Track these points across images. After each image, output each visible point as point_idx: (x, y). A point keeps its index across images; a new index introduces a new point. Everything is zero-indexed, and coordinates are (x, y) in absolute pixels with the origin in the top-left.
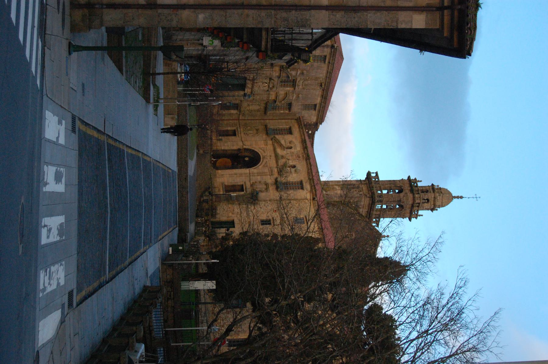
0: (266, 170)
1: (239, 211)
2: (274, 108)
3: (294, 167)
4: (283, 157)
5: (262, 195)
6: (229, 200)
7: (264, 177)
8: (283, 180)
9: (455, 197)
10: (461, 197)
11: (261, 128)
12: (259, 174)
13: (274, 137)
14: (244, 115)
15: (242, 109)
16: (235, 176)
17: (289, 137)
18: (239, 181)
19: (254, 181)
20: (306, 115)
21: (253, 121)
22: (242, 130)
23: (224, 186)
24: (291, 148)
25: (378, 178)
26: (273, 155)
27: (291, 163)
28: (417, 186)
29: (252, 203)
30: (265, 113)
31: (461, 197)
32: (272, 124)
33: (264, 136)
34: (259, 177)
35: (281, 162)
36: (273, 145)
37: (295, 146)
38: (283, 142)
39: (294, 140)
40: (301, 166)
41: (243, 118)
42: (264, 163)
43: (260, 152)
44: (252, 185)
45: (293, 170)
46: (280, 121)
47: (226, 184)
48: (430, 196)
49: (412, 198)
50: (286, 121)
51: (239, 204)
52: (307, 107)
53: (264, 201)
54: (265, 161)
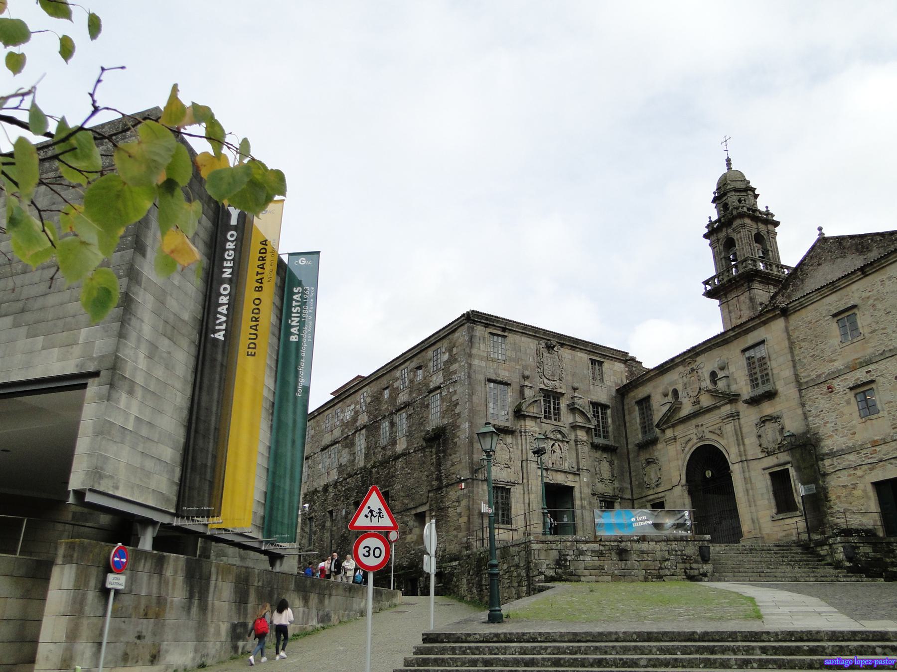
0: (729, 428)
3: (713, 375)
5: (793, 425)
6: (818, 503)
7: (745, 430)
8: (745, 390)
9: (729, 168)
10: (728, 161)
11: (643, 456)
13: (658, 426)
14: (621, 490)
15: (611, 493)
16: (751, 492)
18: (763, 485)
19: (759, 450)
21: (633, 474)
22: (651, 492)
23: (781, 516)
24: (675, 392)
25: (713, 278)
26: (694, 422)
27: (707, 384)
28: (719, 220)
31: (728, 161)
32: (636, 436)
34: (747, 441)
35: (706, 401)
36: (673, 426)
37: (670, 384)
38: (665, 409)
39: (661, 389)
40: (707, 364)
41: (629, 491)
44: (769, 453)
45: (721, 374)
47: (774, 511)
48: (732, 199)
49: (737, 217)
50: (626, 412)
51: (825, 475)
52: (599, 378)
53: (806, 418)
54: (708, 436)
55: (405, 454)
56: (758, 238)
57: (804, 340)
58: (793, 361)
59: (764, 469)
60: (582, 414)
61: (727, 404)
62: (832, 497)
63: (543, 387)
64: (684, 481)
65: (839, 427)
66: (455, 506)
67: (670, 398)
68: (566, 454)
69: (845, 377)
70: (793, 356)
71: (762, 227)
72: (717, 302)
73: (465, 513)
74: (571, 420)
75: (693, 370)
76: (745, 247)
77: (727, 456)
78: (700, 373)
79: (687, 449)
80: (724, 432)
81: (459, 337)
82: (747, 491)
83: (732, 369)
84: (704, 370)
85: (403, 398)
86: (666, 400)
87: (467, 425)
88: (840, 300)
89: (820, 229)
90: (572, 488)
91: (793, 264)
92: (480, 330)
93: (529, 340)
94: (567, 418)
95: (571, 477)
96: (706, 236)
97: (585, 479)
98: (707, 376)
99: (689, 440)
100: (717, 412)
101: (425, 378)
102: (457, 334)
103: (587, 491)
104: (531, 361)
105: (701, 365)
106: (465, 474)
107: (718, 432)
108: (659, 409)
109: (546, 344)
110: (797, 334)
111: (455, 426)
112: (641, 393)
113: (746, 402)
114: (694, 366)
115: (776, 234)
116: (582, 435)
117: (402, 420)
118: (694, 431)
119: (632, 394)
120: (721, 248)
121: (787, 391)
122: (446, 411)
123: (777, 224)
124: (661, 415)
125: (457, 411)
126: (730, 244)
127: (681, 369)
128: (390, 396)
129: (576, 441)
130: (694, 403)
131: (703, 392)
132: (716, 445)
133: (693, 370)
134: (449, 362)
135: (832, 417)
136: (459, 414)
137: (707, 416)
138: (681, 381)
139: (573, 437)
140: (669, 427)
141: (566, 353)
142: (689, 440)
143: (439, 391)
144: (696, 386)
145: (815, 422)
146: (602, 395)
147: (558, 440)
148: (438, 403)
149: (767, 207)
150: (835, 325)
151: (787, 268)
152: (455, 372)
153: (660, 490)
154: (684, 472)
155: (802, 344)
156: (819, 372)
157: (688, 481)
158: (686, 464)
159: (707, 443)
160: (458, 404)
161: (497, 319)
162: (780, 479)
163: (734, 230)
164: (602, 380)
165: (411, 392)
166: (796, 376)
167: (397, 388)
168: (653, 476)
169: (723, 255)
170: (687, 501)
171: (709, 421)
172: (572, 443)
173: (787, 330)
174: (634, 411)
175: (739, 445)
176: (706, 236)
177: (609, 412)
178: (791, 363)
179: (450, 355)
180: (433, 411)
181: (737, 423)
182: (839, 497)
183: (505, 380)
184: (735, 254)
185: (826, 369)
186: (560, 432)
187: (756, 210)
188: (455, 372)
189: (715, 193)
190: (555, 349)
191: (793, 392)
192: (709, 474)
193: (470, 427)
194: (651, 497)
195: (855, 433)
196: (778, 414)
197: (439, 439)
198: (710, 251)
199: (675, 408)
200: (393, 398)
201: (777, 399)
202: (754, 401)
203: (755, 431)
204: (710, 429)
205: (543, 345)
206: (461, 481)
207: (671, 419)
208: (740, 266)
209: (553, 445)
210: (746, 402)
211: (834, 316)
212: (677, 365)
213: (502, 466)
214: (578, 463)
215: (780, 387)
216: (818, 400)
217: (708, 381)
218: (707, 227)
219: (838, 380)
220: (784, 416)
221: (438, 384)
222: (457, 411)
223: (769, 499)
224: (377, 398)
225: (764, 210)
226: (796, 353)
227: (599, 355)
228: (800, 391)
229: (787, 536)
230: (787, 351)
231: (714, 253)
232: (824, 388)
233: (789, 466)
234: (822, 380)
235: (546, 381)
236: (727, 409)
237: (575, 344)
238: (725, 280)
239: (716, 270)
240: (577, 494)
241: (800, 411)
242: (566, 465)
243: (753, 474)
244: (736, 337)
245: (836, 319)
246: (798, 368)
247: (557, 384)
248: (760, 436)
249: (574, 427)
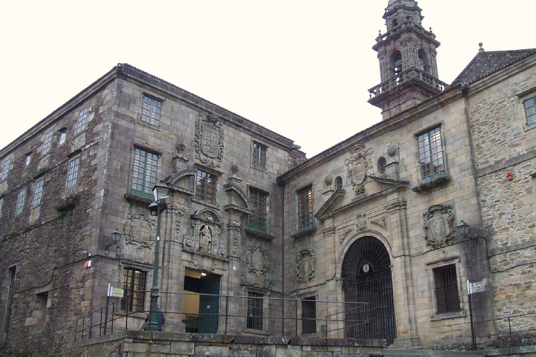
0: (394, 218)
1: (519, 270)
2: (261, 222)
3: (382, 161)
4: (361, 191)
7: (411, 221)
11: (299, 247)
12: (404, 231)
15: (261, 285)
17: (319, 187)
18: (425, 281)
19: (424, 243)
20: (277, 166)
21: (286, 266)
22: (302, 286)
23: (442, 316)
24: (339, 180)
25: (378, 86)
26: (356, 212)
27: (374, 171)
29: (487, 240)
30: (268, 240)
33: (317, 238)
34: (412, 234)
35: (371, 189)
36: (333, 217)
37: (334, 172)
38: (326, 198)
39: (323, 179)
41: (280, 285)
43: (349, 241)
46: (286, 215)
47: (434, 310)
52: (260, 162)
54: (370, 227)
55: (38, 225)
56: (422, 54)
57: (483, 124)
58: (471, 145)
59: (428, 264)
61: (395, 191)
62: (501, 297)
63: (198, 161)
64: (338, 276)
65: (516, 219)
66: (78, 288)
67: (333, 187)
68: (216, 239)
69: (528, 163)
70: (471, 141)
71: (425, 45)
72: (380, 110)
73: (88, 295)
74: (226, 203)
75: (360, 156)
76: (410, 60)
77: (388, 249)
78: (367, 160)
79: (346, 241)
80: (388, 224)
81: (107, 94)
82: (407, 288)
83: (403, 155)
84: (372, 156)
85: (44, 164)
86: (329, 188)
87: (102, 193)
88: (528, 79)
89: (481, 45)
90: (219, 276)
91: (449, 82)
92: (131, 89)
93: (189, 110)
94: (222, 200)
95: (219, 265)
96: (375, 48)
97: (234, 268)
98: (374, 162)
99: (350, 231)
101: (67, 141)
102: (106, 91)
103: (235, 281)
104: (189, 133)
105: (370, 152)
106: (93, 250)
107: (381, 222)
108: (320, 196)
109: (208, 117)
110: (477, 116)
111: (89, 195)
112: (301, 182)
113: (416, 190)
114: (362, 152)
115: (436, 53)
116: (236, 220)
117: (38, 189)
118: (356, 222)
119: (293, 183)
120: (388, 59)
121: (462, 179)
122: (83, 177)
123: (437, 44)
124: (321, 204)
125: (94, 178)
126: (396, 56)
127: (348, 155)
128: (32, 162)
129: (229, 226)
130: (358, 192)
131: (369, 179)
132: (378, 237)
133: (360, 156)
134: (94, 123)
135: (508, 208)
136: (96, 181)
137: (370, 206)
138: (346, 168)
139: (226, 221)
140: (329, 217)
141: (229, 132)
142: (350, 231)
143: (79, 155)
144: (362, 173)
145: (488, 213)
146: (264, 183)
147: (208, 222)
148: (77, 168)
149: (430, 28)
150: (521, 106)
151: (444, 84)
152: (97, 134)
153: (313, 283)
154: (341, 263)
155: (482, 128)
156: (499, 158)
158: (343, 257)
159: (368, 234)
160: (95, 169)
161: (154, 79)
162: (445, 276)
163: (401, 43)
164: (263, 165)
165: (52, 158)
166: (473, 161)
167: (40, 154)
168: (306, 267)
169: (389, 66)
170: (340, 296)
171: (374, 210)
172: (225, 227)
173: (466, 112)
174: (294, 200)
175: (403, 238)
176: (375, 48)
177: (268, 199)
178: (469, 148)
179: (96, 114)
180: (70, 178)
181: (403, 214)
182: (509, 297)
183: (156, 148)
184: (400, 66)
185: (506, 154)
186: (213, 214)
187: (421, 28)
188: (97, 134)
189: (386, 9)
190: (218, 124)
191: (468, 180)
192: (366, 268)
193: (105, 195)
194: (302, 292)
195: (533, 226)
196: (450, 203)
197: (71, 208)
198: (376, 63)
200: (34, 163)
201: (450, 188)
202: (424, 190)
203: (422, 222)
204: (373, 219)
205: (204, 117)
206: (89, 258)
207: (331, 209)
208: (404, 76)
209: (203, 227)
210: (416, 190)
211: (521, 96)
212: (343, 151)
213: (139, 245)
214: (228, 250)
215: (454, 173)
216: (495, 188)
217: (375, 169)
218: (377, 40)
219: (520, 166)
220: (456, 205)
221: (79, 148)
222: (94, 178)
223: (430, 298)
224: (19, 165)
225: (429, 30)
226: (474, 137)
227: (265, 140)
228: (476, 178)
229: (446, 338)
230: (465, 134)
231: (381, 64)
232: (503, 176)
233: (456, 261)
234: (501, 166)
235: (203, 157)
236: (393, 198)
237: (239, 123)
238: (389, 89)
239: (382, 80)
240: (224, 283)
241: (474, 201)
242: (216, 250)
243: (415, 269)
244: (410, 120)
245: (522, 100)
246: (476, 153)
247: (215, 162)
248: (426, 228)
249: (229, 210)
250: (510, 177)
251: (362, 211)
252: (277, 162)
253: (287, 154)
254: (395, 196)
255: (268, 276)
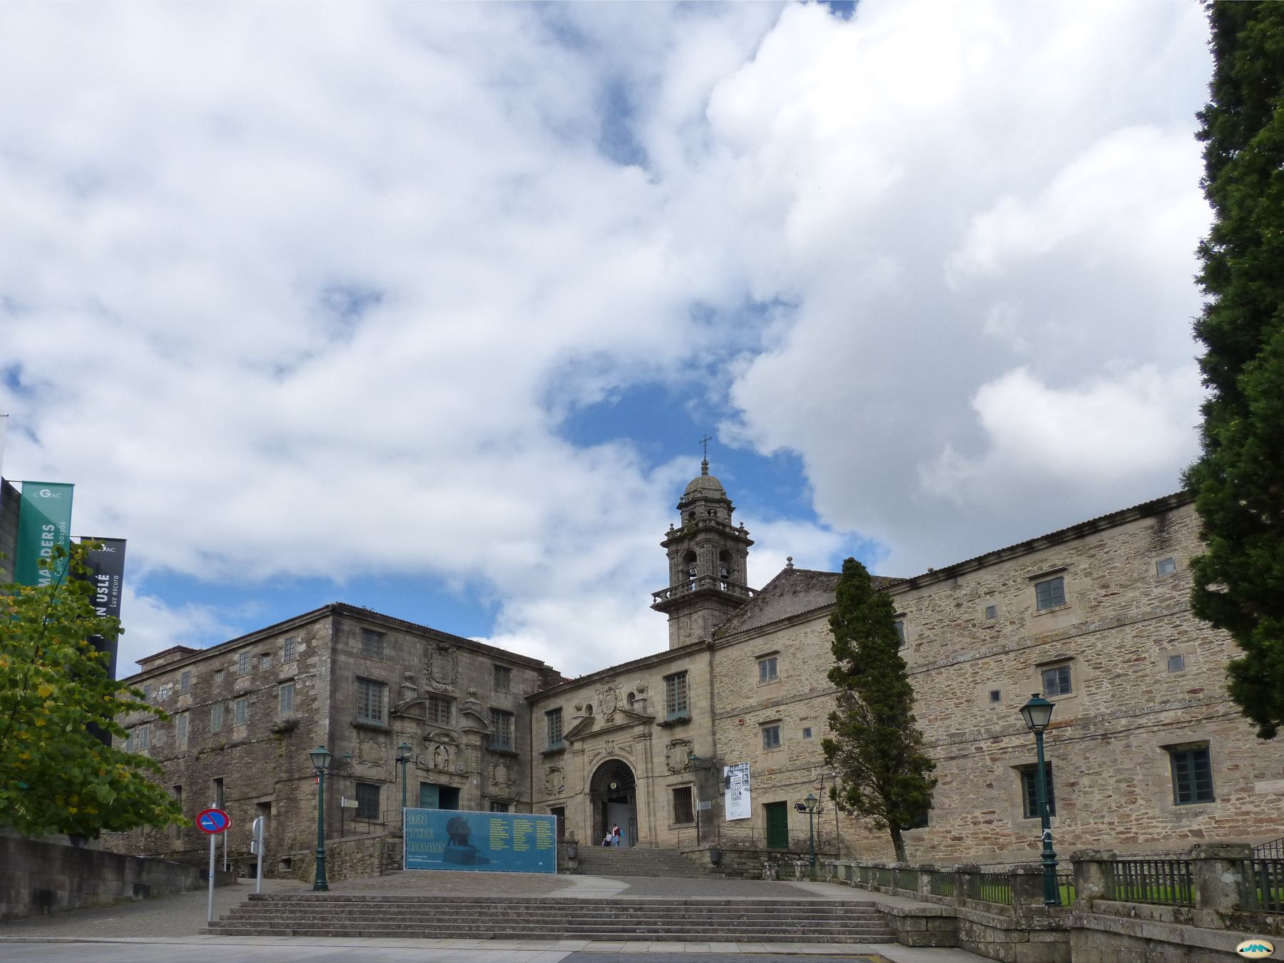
0: (639, 747)
5: (701, 750)
7: (655, 750)
12: (649, 756)
24: (590, 708)
34: (655, 760)
36: (583, 740)
42: (623, 753)
44: (675, 772)
54: (617, 751)
60: (478, 719)
64: (587, 790)
95: (457, 779)
100: (630, 731)
108: (570, 721)
130: (608, 721)
137: (619, 734)
157: (591, 790)
168: (555, 782)
171: (622, 739)
192: (613, 786)
199: (589, 721)
236: (639, 730)
241: (710, 739)
243: (657, 789)
250: (742, 722)
251: (610, 737)
252: (522, 684)
253: (535, 674)
254: (641, 728)
255: (514, 789)
